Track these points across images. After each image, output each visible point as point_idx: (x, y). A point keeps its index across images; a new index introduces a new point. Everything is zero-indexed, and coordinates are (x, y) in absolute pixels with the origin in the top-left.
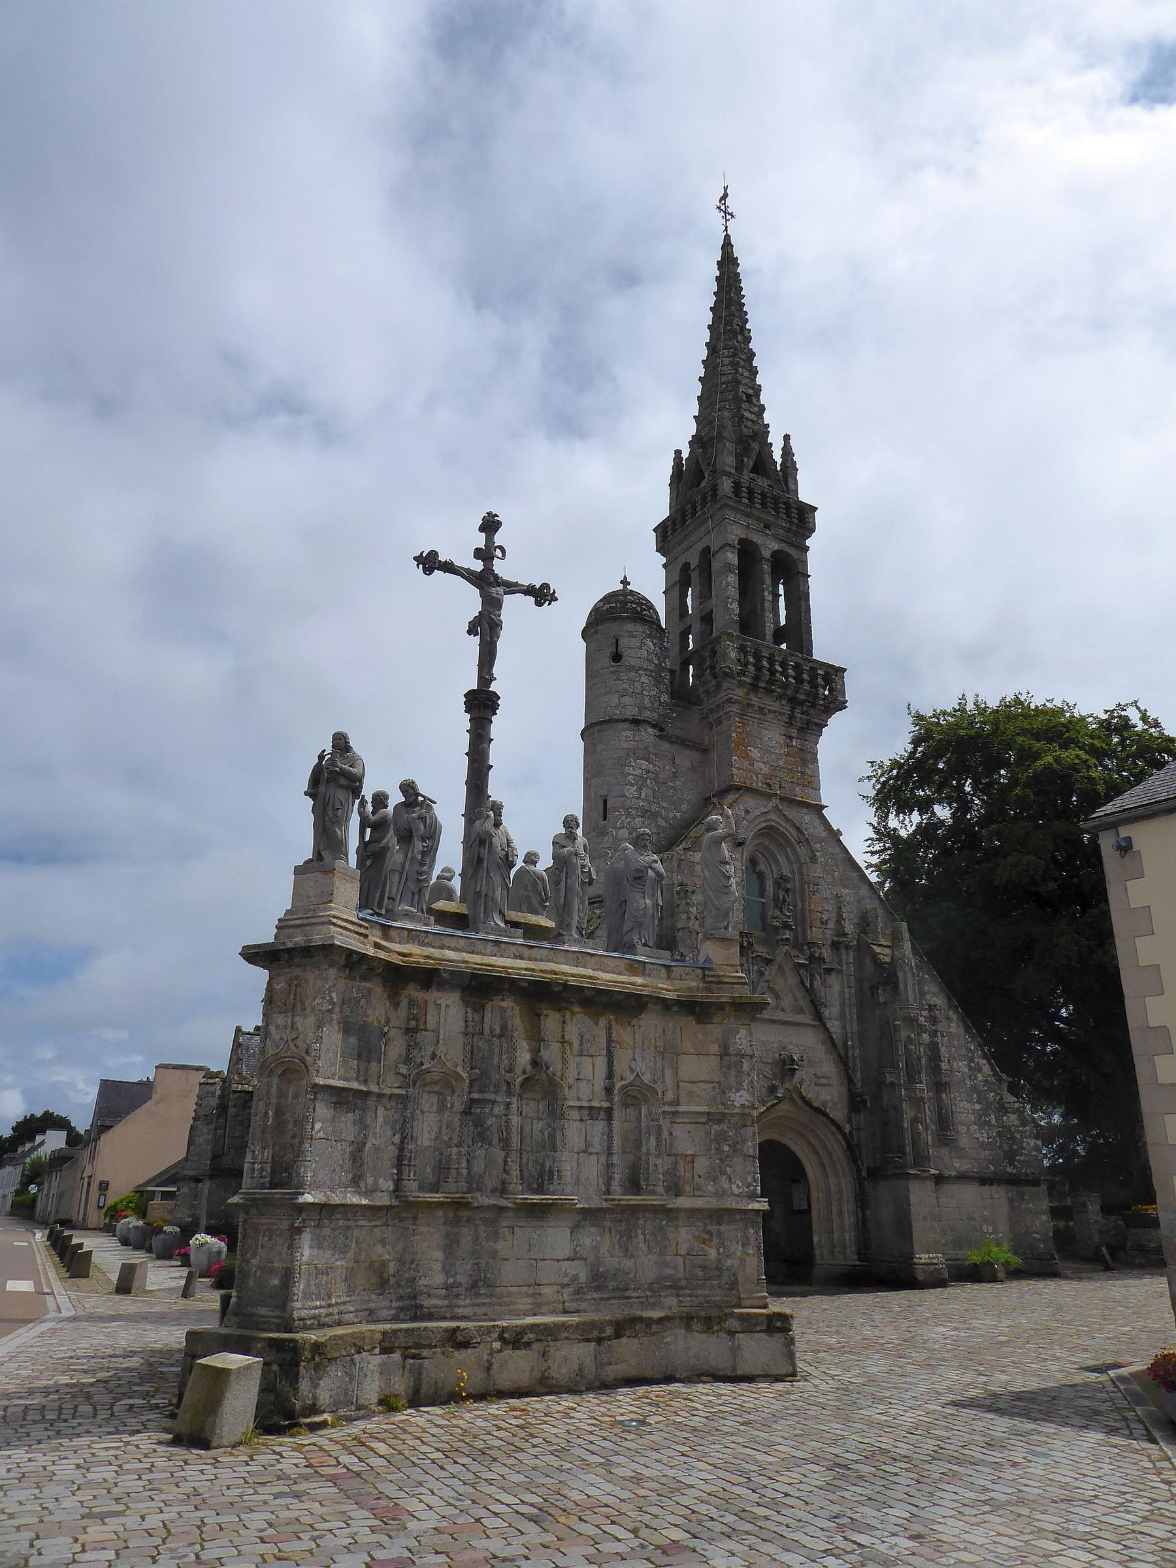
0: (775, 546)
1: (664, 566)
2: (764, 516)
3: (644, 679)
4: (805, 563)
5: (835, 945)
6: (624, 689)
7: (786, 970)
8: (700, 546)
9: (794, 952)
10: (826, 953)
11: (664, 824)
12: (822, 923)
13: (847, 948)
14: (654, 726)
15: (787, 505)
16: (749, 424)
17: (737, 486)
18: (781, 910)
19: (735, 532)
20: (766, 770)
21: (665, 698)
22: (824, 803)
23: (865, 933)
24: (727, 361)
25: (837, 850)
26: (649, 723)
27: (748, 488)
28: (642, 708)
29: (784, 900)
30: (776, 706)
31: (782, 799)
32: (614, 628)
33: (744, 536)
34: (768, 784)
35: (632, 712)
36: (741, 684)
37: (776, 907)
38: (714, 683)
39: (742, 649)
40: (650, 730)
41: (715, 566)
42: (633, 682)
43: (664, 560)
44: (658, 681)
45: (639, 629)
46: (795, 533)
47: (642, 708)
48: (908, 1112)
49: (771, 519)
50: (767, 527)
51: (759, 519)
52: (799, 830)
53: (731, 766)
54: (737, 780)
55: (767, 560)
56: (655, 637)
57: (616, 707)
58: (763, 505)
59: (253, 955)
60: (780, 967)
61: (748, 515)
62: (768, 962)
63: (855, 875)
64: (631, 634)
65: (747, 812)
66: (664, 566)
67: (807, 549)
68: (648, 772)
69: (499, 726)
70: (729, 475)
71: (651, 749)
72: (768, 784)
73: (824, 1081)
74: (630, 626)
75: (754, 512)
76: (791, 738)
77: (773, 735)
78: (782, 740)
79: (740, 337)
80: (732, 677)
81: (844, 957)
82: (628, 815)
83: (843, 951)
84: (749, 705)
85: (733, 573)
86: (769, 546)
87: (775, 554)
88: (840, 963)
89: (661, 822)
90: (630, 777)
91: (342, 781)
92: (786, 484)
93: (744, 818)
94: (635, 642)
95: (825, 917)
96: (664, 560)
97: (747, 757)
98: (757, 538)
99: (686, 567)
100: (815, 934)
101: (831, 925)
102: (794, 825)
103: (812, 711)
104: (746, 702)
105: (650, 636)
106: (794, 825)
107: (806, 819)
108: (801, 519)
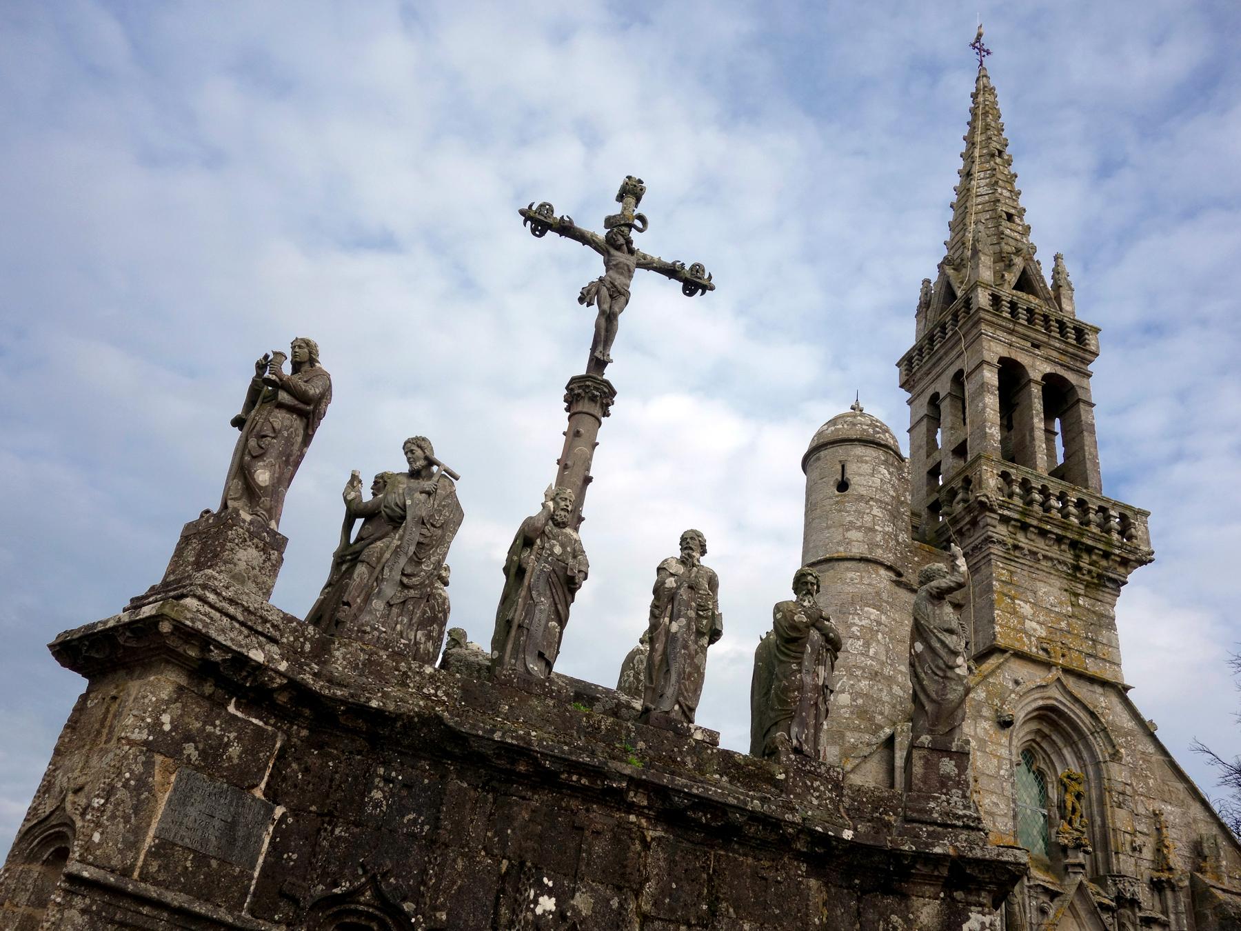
0: (1048, 369)
1: (910, 402)
2: (1033, 335)
3: (876, 511)
4: (1087, 390)
5: (1157, 886)
6: (850, 522)
7: (1082, 914)
9: (1092, 888)
10: (1143, 894)
11: (901, 694)
12: (1134, 849)
13: (1173, 888)
14: (889, 568)
15: (1062, 326)
16: (1012, 242)
17: (996, 300)
18: (1070, 823)
19: (994, 348)
20: (1042, 632)
21: (904, 537)
22: (1127, 682)
23: (1201, 870)
24: (983, 182)
25: (1151, 749)
26: (882, 564)
27: (1010, 302)
28: (872, 545)
29: (1074, 810)
30: (1054, 552)
31: (1067, 671)
32: (840, 451)
33: (1006, 355)
34: (1045, 650)
35: (856, 551)
36: (1005, 520)
37: (1063, 817)
38: (967, 519)
39: (1005, 476)
40: (882, 572)
41: (969, 388)
42: (860, 514)
44: (894, 516)
45: (870, 453)
46: (1074, 357)
47: (872, 545)
49: (1040, 337)
51: (1025, 337)
52: (1092, 715)
53: (992, 621)
54: (1001, 642)
55: (1037, 382)
56: (892, 465)
57: (839, 543)
58: (1030, 321)
60: (1072, 905)
61: (1012, 332)
62: (1053, 895)
63: (1181, 786)
64: (860, 460)
65: (1017, 683)
66: (910, 402)
67: (1089, 376)
68: (879, 623)
69: (610, 433)
70: (986, 286)
71: (885, 596)
72: (1045, 650)
74: (859, 450)
76: (1077, 595)
77: (1051, 591)
78: (1065, 597)
79: (998, 160)
80: (994, 511)
81: (1170, 903)
82: (851, 675)
83: (1169, 894)
84: (1016, 547)
85: (992, 393)
86: (1038, 368)
87: (1046, 377)
88: (1165, 912)
90: (854, 629)
91: (283, 396)
92: (1060, 305)
93: (1013, 691)
94: (866, 468)
95: (1138, 842)
96: (909, 396)
97: (1014, 612)
98: (1023, 359)
99: (934, 400)
100: (1125, 864)
101: (1147, 854)
102: (1085, 708)
103: (1104, 563)
104: (1010, 541)
105: (885, 462)
106: (1085, 708)
107: (1103, 701)
108: (1078, 340)
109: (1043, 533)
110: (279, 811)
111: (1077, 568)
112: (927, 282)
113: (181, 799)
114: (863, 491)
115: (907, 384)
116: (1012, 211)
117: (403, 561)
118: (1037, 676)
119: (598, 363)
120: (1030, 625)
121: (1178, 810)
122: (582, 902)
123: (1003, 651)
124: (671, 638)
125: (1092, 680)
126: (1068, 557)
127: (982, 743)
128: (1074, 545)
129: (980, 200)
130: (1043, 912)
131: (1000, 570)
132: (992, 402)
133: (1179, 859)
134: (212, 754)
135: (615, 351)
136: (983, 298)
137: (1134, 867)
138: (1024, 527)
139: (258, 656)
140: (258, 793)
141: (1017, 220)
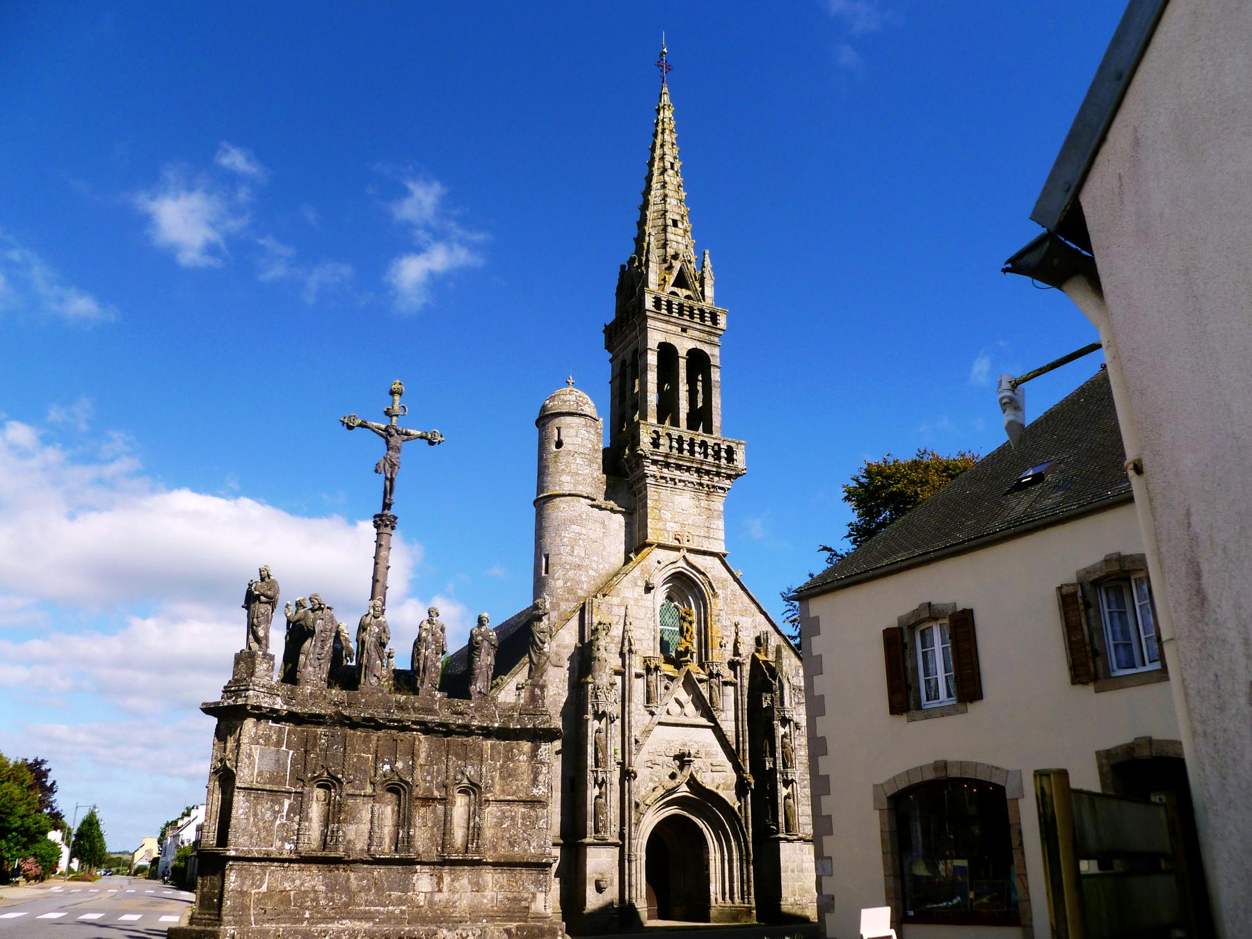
0: (692, 345)
1: (611, 361)
3: (579, 461)
5: (733, 665)
8: (631, 348)
15: (702, 312)
17: (658, 302)
28: (577, 484)
30: (685, 476)
31: (690, 551)
36: (655, 462)
43: (610, 356)
46: (709, 333)
48: (783, 792)
50: (684, 330)
54: (650, 539)
59: (209, 710)
61: (667, 322)
62: (671, 679)
63: (753, 606)
66: (611, 361)
70: (652, 292)
73: (718, 768)
74: (568, 419)
75: (673, 320)
84: (662, 478)
86: (683, 346)
89: (591, 572)
91: (263, 598)
94: (572, 432)
96: (610, 356)
97: (660, 519)
99: (623, 363)
101: (730, 647)
109: (679, 467)
110: (291, 752)
111: (701, 484)
112: (623, 267)
113: (262, 756)
114: (570, 448)
115: (609, 347)
116: (677, 217)
117: (317, 650)
118: (673, 555)
119: (386, 506)
120: (670, 525)
121: (750, 620)
122: (400, 765)
123: (651, 545)
124: (426, 658)
125: (705, 553)
126: (694, 477)
127: (637, 600)
128: (698, 471)
129: (656, 208)
130: (667, 688)
131: (651, 492)
132: (652, 377)
133: (747, 649)
134: (268, 738)
135: (395, 497)
136: (649, 303)
137: (721, 656)
138: (667, 465)
139: (276, 707)
140: (284, 748)
141: (680, 225)
